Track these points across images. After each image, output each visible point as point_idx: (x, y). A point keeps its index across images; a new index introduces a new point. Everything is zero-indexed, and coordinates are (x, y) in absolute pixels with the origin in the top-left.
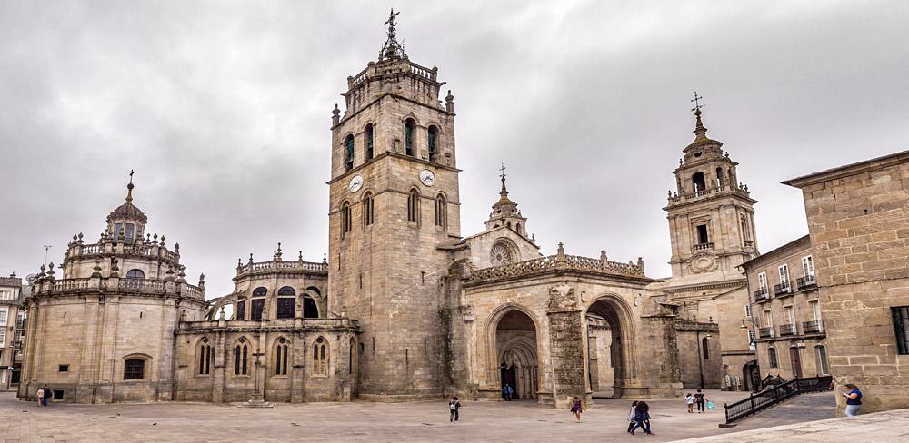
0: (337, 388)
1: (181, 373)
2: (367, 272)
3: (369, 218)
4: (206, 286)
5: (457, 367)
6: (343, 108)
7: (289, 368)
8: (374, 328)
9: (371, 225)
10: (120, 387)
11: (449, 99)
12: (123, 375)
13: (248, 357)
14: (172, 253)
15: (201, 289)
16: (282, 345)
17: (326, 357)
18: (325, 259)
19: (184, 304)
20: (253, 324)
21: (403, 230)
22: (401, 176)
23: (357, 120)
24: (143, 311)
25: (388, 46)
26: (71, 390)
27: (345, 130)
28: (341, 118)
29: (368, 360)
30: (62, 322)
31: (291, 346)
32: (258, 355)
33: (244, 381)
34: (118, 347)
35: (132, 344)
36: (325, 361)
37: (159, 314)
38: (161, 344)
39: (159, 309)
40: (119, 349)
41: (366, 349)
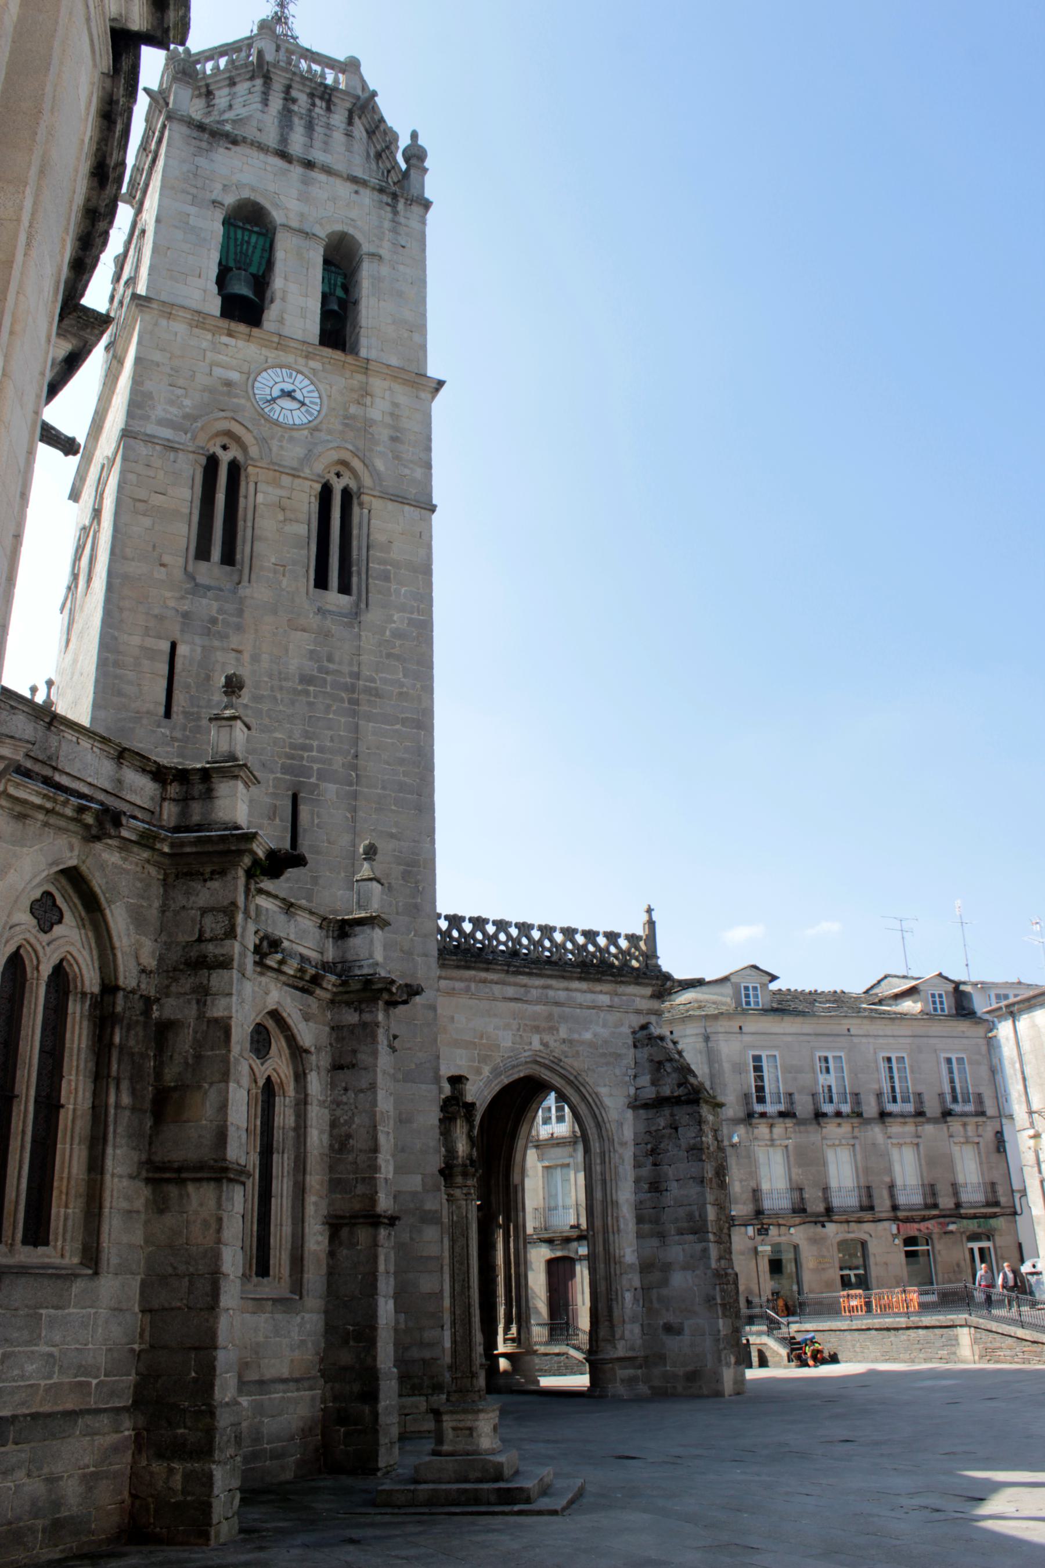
2: (331, 790)
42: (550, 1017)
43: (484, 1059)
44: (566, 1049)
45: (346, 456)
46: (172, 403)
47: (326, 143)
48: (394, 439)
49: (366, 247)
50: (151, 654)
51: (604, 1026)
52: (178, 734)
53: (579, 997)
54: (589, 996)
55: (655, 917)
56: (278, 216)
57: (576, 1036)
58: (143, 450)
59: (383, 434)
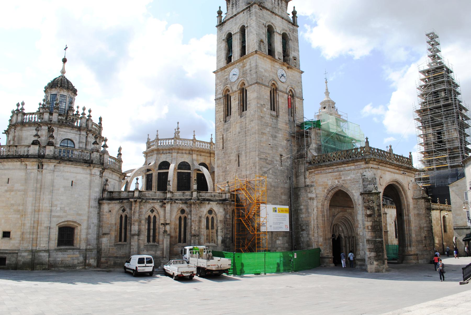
1: (105, 240)
2: (243, 152)
3: (243, 106)
4: (123, 157)
6: (224, 10)
7: (188, 237)
11: (294, 13)
12: (57, 241)
13: (157, 226)
14: (96, 125)
15: (119, 161)
17: (215, 227)
18: (212, 139)
19: (107, 174)
20: (159, 194)
21: (268, 118)
22: (265, 71)
23: (234, 22)
27: (227, 28)
28: (223, 18)
30: (6, 188)
31: (189, 217)
32: (165, 224)
33: (154, 249)
34: (53, 214)
35: (65, 212)
37: (87, 183)
38: (89, 212)
40: (54, 217)
42: (340, 175)
43: (325, 188)
44: (344, 182)
45: (243, 81)
46: (220, 89)
48: (250, 71)
49: (246, 26)
52: (224, 151)
53: (347, 168)
54: (349, 167)
55: (369, 140)
56: (232, 34)
57: (346, 179)
58: (217, 101)
59: (248, 71)
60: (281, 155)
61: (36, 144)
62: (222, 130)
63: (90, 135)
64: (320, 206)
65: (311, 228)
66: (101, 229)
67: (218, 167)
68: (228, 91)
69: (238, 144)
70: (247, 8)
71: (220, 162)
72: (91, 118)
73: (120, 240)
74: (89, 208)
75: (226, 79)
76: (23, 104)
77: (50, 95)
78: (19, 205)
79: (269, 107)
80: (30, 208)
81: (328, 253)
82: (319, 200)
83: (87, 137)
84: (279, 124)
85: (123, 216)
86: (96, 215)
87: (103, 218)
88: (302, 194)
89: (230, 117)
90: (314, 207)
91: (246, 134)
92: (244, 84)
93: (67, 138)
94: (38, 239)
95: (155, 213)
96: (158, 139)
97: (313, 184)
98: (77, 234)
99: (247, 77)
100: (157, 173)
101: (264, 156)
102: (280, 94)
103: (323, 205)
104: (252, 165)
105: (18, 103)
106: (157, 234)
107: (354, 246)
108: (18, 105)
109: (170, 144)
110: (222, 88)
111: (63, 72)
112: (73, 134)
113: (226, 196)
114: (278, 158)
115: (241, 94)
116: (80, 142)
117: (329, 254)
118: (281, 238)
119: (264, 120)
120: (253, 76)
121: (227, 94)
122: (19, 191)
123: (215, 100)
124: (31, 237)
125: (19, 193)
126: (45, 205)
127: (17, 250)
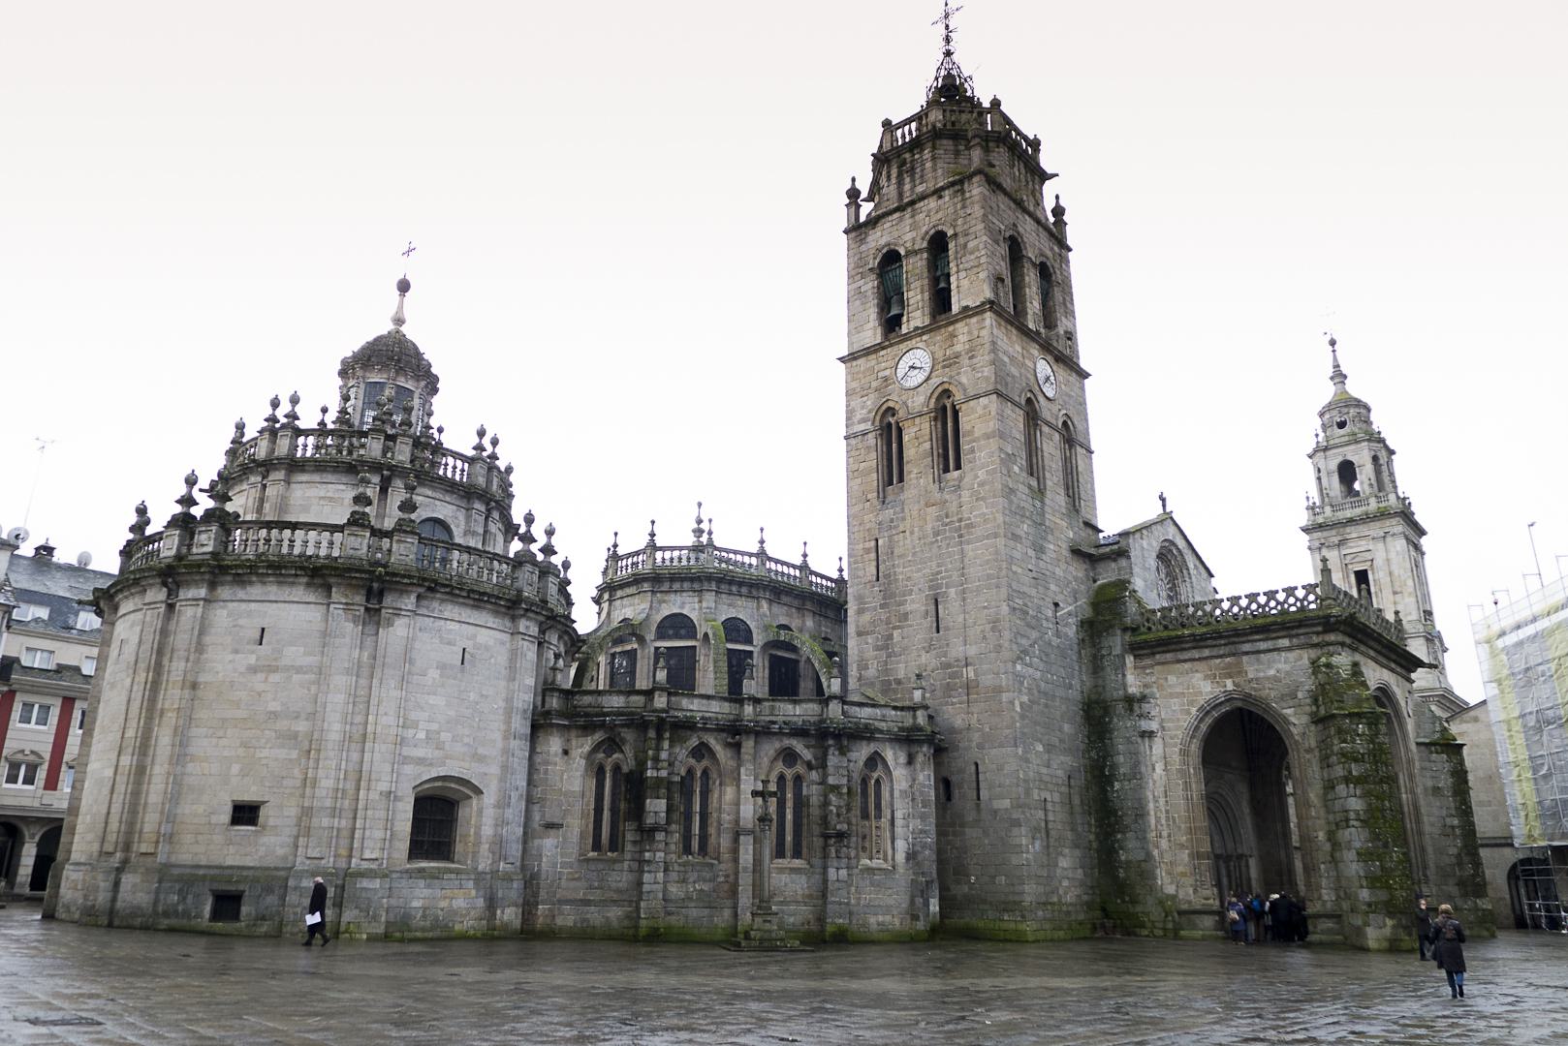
0: (912, 902)
2: (952, 591)
3: (949, 453)
5: (1129, 851)
8: (976, 737)
9: (956, 473)
10: (404, 882)
11: (1058, 211)
16: (789, 773)
17: (886, 813)
24: (469, 645)
25: (943, 73)
26: (269, 890)
29: (962, 825)
30: (252, 659)
35: (440, 746)
36: (885, 822)
37: (502, 659)
39: (503, 643)
40: (406, 760)
41: (956, 793)
43: (1191, 703)
45: (946, 386)
46: (863, 408)
47: (922, 176)
48: (970, 358)
50: (867, 551)
51: (1285, 662)
56: (903, 253)
57: (1262, 674)
58: (853, 442)
60: (1056, 605)
61: (363, 526)
62: (873, 525)
63: (496, 515)
64: (1176, 758)
65: (1149, 822)
66: (536, 808)
67: (859, 634)
68: (890, 413)
69: (934, 567)
70: (953, 184)
71: (866, 617)
72: (497, 462)
73: (597, 846)
74: (506, 738)
75: (886, 379)
76: (295, 400)
77: (362, 386)
78: (297, 718)
79: (1024, 463)
80: (334, 730)
81: (1207, 899)
82: (1172, 738)
83: (487, 518)
84: (1047, 516)
85: (608, 769)
86: (526, 763)
87: (546, 772)
88: (1115, 720)
89: (902, 489)
90: (1154, 758)
91: (960, 536)
92: (947, 393)
93: (434, 515)
94: (357, 831)
95: (705, 763)
96: (652, 547)
97: (1147, 691)
98: (468, 823)
99: (959, 374)
100: (652, 650)
101: (1020, 602)
102: (1046, 429)
103: (1184, 753)
104: (988, 627)
105: (276, 398)
106: (712, 830)
107: (1244, 882)
108: (275, 404)
109: (668, 563)
110: (871, 402)
111: (399, 321)
112: (450, 507)
113: (915, 717)
114: (1050, 613)
115: (939, 426)
116: (467, 532)
117: (1211, 901)
118: (1067, 851)
119: (1015, 500)
120: (982, 372)
121: (885, 421)
122: (299, 670)
123: (846, 438)
124: (336, 825)
125: (296, 678)
126: (385, 720)
127: (283, 869)
